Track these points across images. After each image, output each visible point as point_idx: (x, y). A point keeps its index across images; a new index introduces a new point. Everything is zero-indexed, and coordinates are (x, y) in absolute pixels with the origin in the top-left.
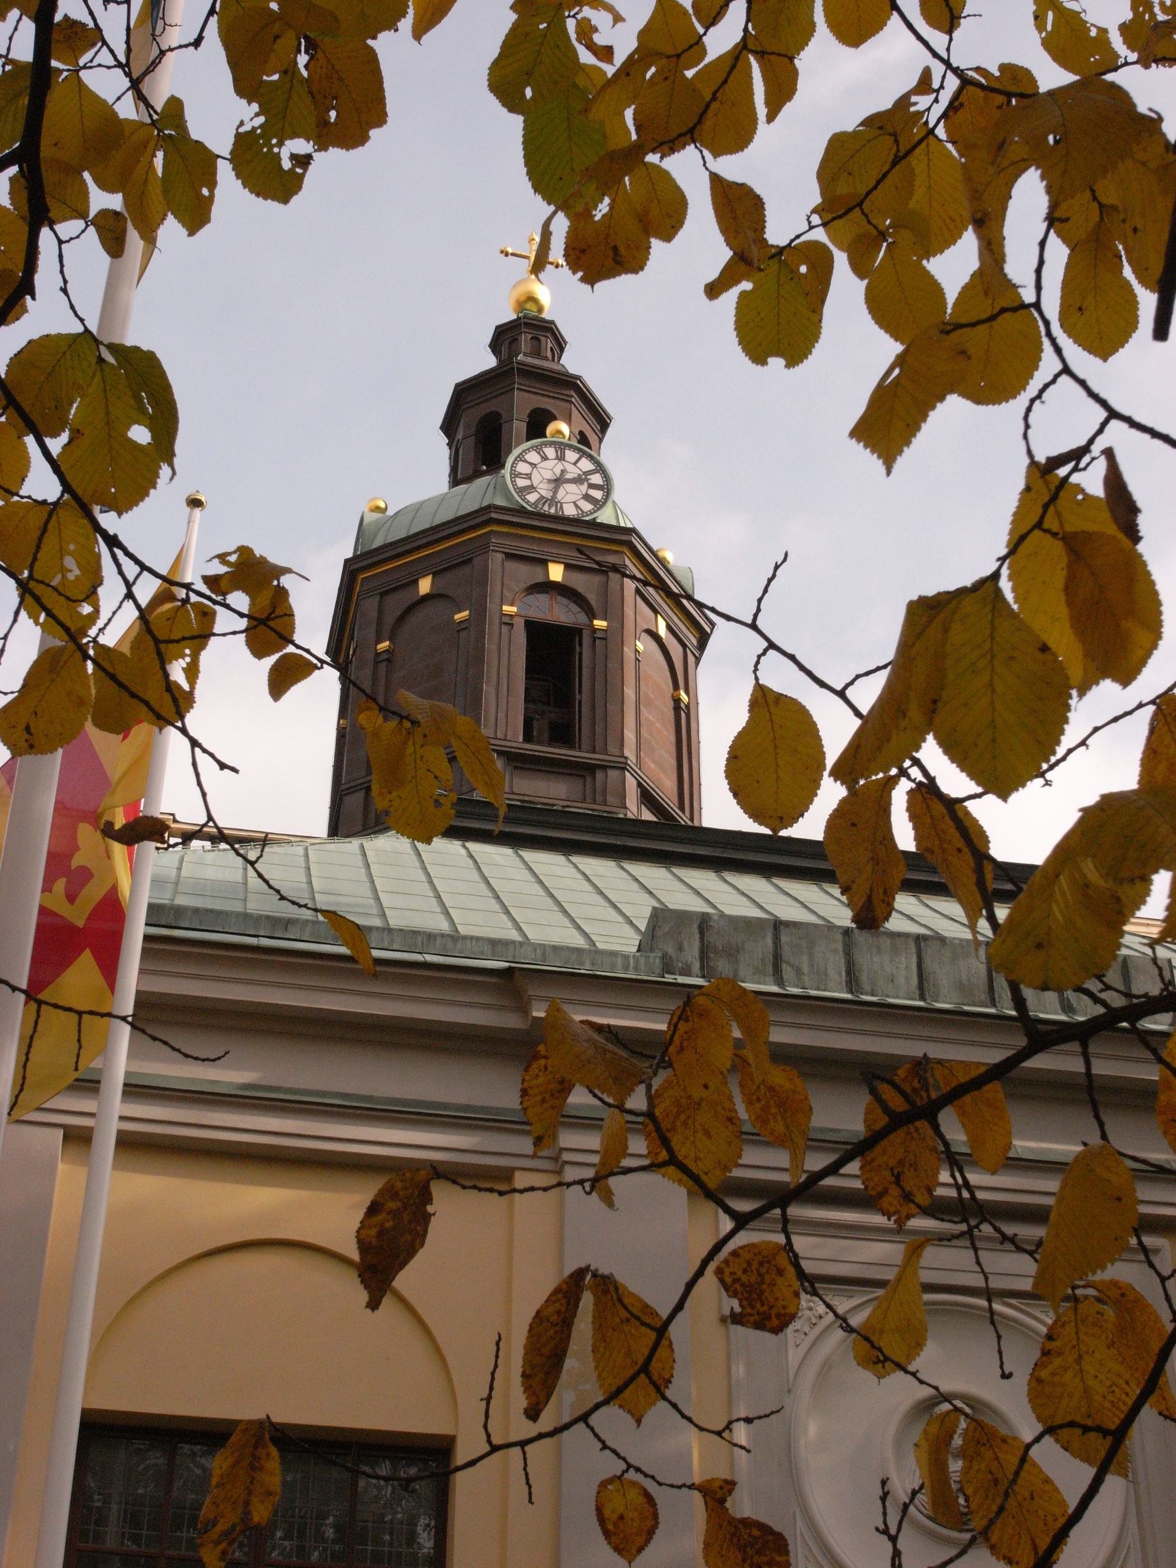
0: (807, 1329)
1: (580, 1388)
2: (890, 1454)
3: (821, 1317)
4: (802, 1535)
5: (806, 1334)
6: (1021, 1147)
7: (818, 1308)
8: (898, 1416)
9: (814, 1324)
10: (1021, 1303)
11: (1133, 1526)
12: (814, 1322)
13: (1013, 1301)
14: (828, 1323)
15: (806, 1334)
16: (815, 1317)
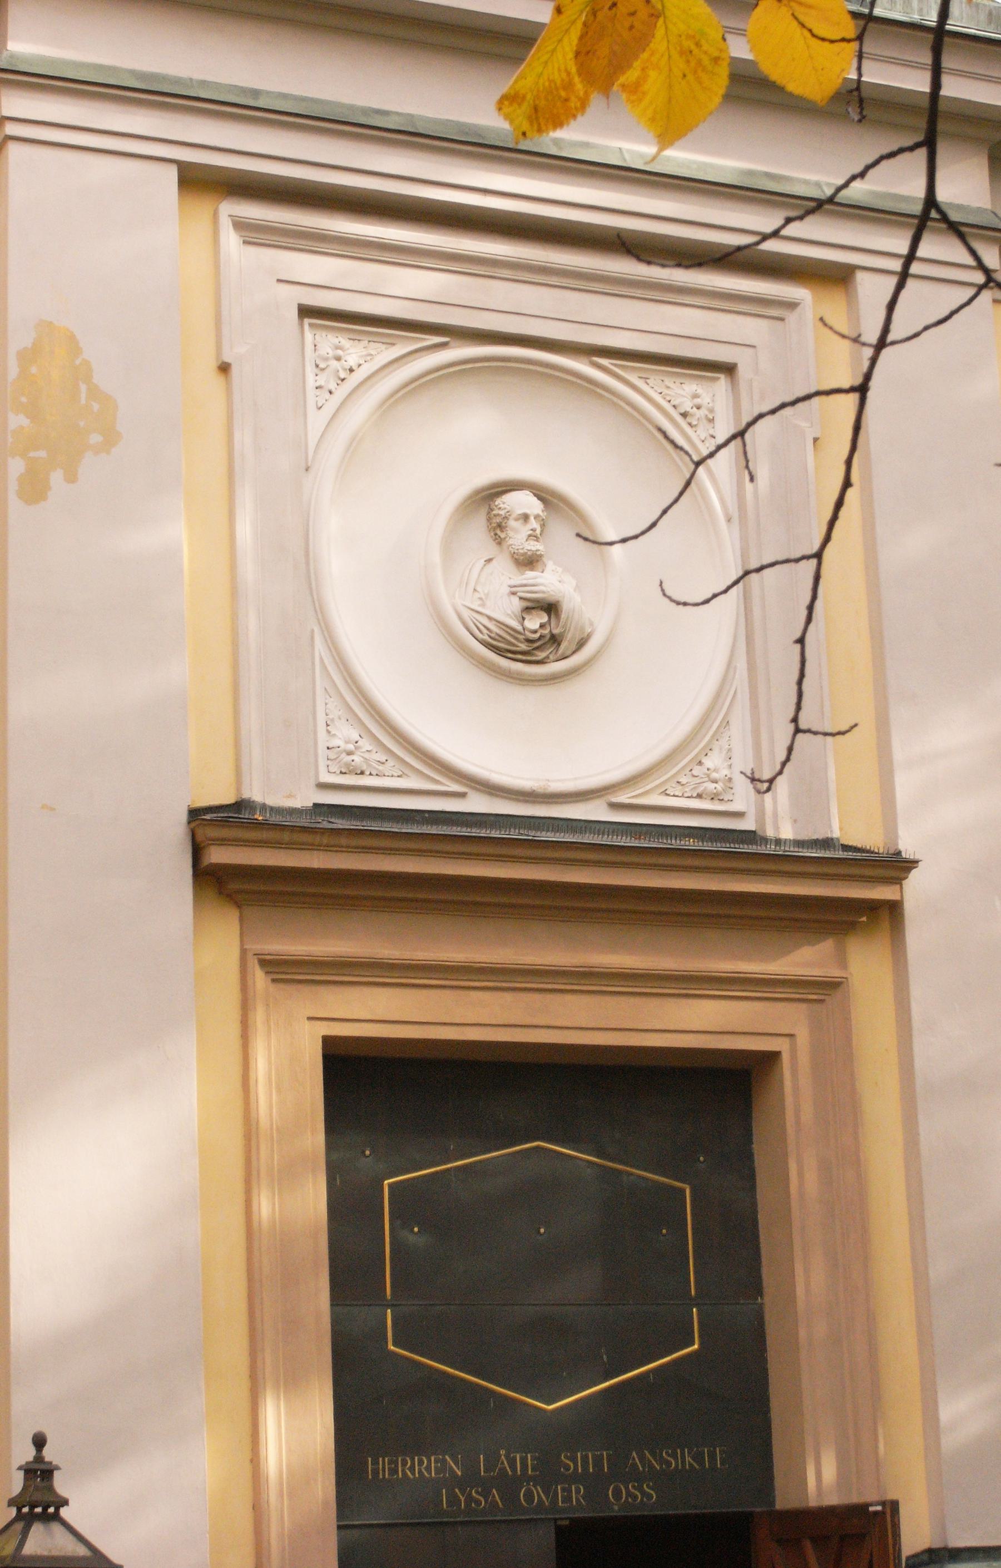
0: (332, 386)
1: (32, 454)
2: (436, 558)
3: (351, 370)
4: (321, 660)
5: (331, 392)
6: (628, 151)
7: (348, 358)
8: (448, 508)
9: (343, 380)
10: (615, 365)
11: (741, 664)
12: (342, 377)
13: (605, 362)
14: (361, 379)
15: (331, 392)
16: (345, 370)
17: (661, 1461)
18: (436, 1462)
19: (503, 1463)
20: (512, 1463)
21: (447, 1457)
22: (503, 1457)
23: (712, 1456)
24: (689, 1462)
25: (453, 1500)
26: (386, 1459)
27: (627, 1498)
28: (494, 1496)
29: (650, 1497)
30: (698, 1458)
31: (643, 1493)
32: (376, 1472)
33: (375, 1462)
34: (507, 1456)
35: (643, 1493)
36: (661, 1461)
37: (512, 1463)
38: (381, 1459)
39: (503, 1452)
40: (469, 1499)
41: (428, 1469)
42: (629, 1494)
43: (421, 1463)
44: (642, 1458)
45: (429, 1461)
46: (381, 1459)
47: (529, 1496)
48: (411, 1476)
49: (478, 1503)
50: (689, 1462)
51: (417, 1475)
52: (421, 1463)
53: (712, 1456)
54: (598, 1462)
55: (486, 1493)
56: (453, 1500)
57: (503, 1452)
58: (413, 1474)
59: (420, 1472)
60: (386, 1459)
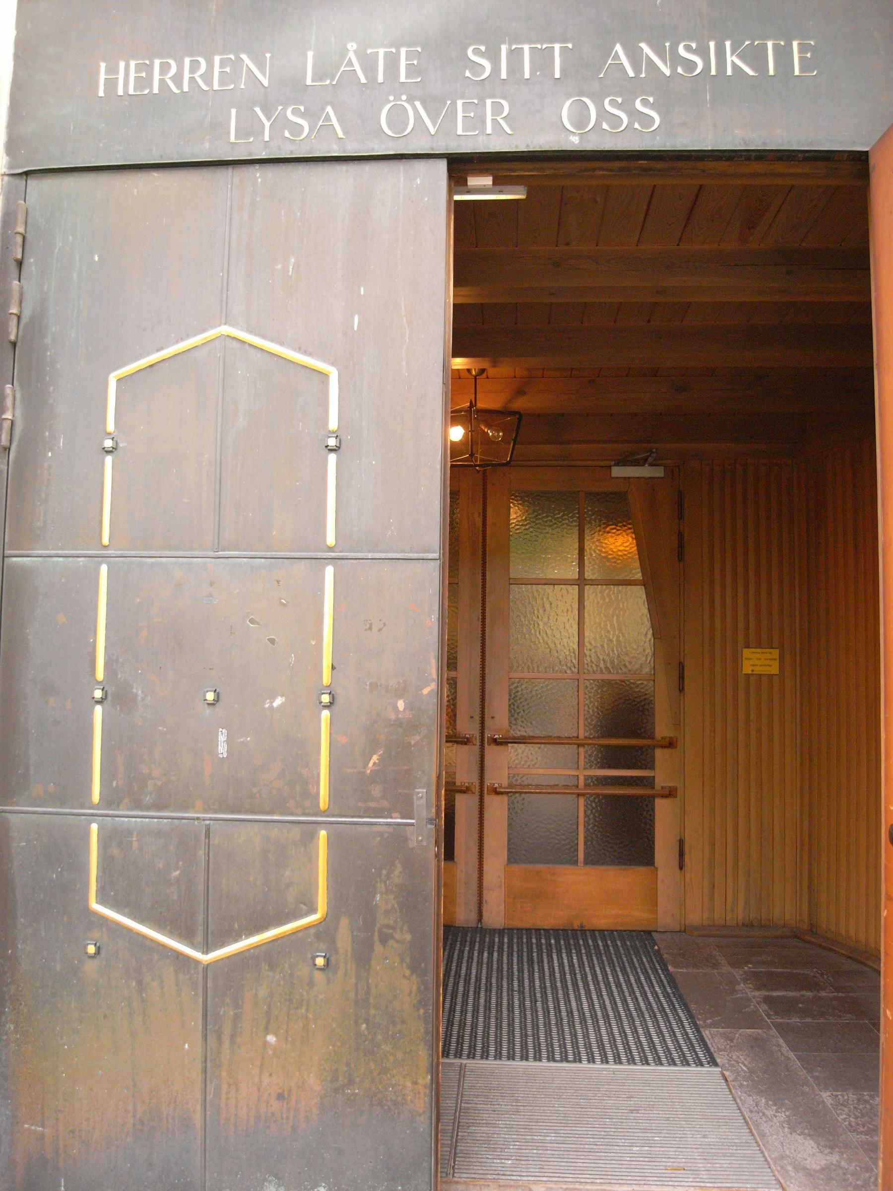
17: (676, 60)
18: (223, 63)
19: (350, 63)
20: (369, 65)
21: (244, 56)
22: (351, 55)
23: (783, 54)
24: (733, 63)
25: (249, 128)
26: (133, 64)
27: (598, 123)
28: (328, 118)
29: (647, 120)
30: (756, 57)
31: (634, 114)
32: (111, 84)
33: (112, 69)
34: (362, 56)
35: (634, 114)
36: (676, 60)
37: (369, 65)
38: (122, 65)
39: (352, 46)
40: (281, 124)
41: (207, 77)
42: (602, 114)
43: (195, 66)
44: (635, 57)
45: (210, 66)
46: (122, 65)
47: (397, 118)
48: (176, 90)
49: (296, 129)
50: (733, 63)
51: (186, 89)
52: (195, 66)
53: (783, 54)
54: (543, 60)
55: (311, 114)
56: (249, 128)
57: (352, 46)
58: (179, 85)
59: (192, 80)
60: (133, 64)
